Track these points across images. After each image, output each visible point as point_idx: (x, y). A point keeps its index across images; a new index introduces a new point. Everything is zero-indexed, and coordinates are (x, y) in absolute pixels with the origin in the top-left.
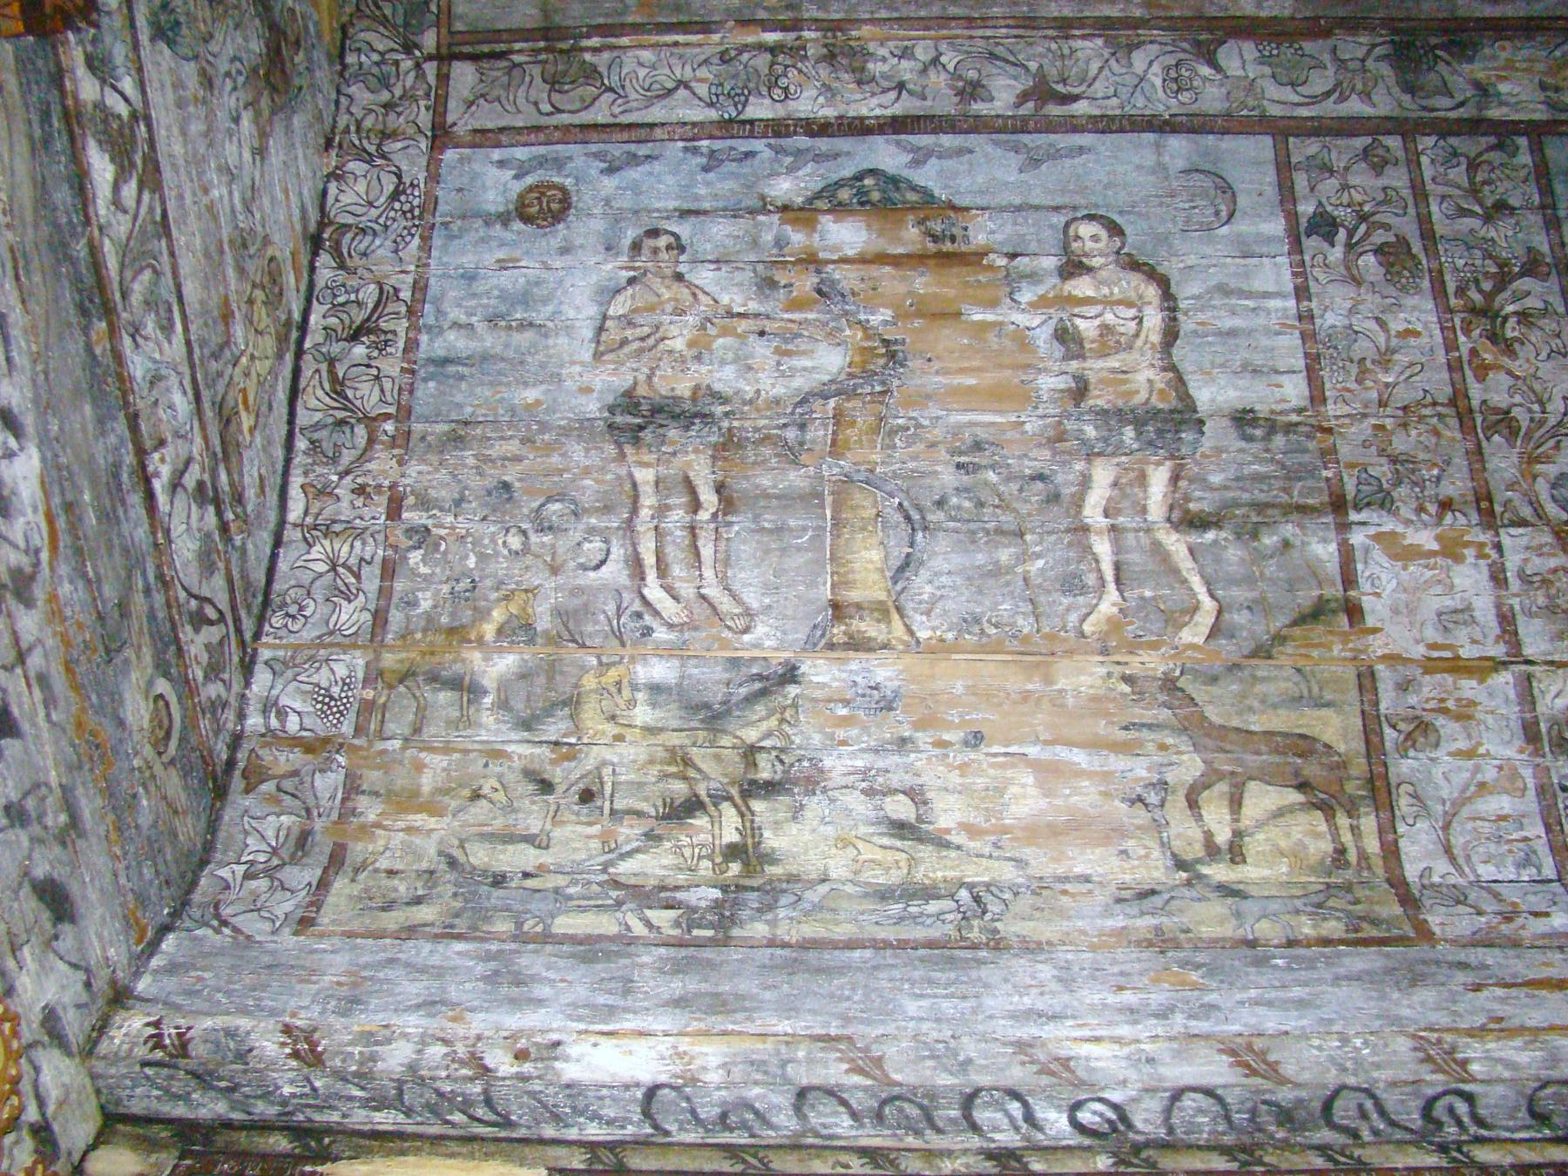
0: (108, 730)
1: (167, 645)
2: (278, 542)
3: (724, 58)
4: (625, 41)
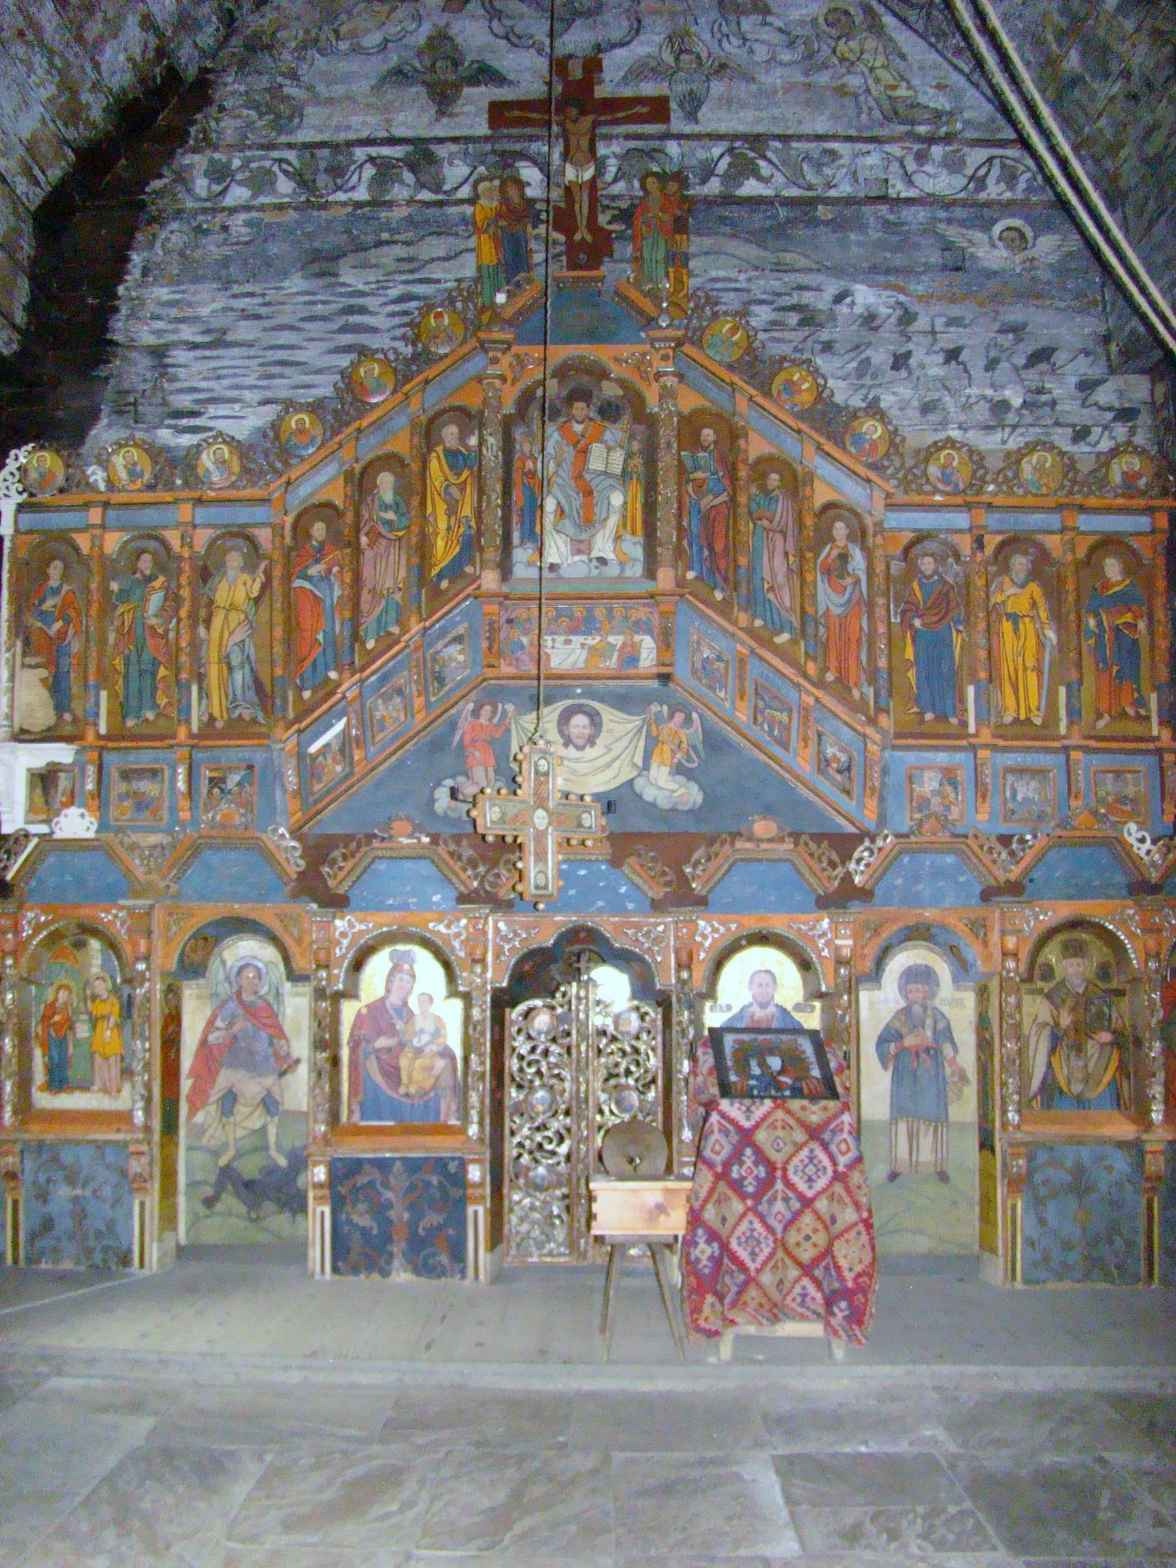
0: (993, 285)
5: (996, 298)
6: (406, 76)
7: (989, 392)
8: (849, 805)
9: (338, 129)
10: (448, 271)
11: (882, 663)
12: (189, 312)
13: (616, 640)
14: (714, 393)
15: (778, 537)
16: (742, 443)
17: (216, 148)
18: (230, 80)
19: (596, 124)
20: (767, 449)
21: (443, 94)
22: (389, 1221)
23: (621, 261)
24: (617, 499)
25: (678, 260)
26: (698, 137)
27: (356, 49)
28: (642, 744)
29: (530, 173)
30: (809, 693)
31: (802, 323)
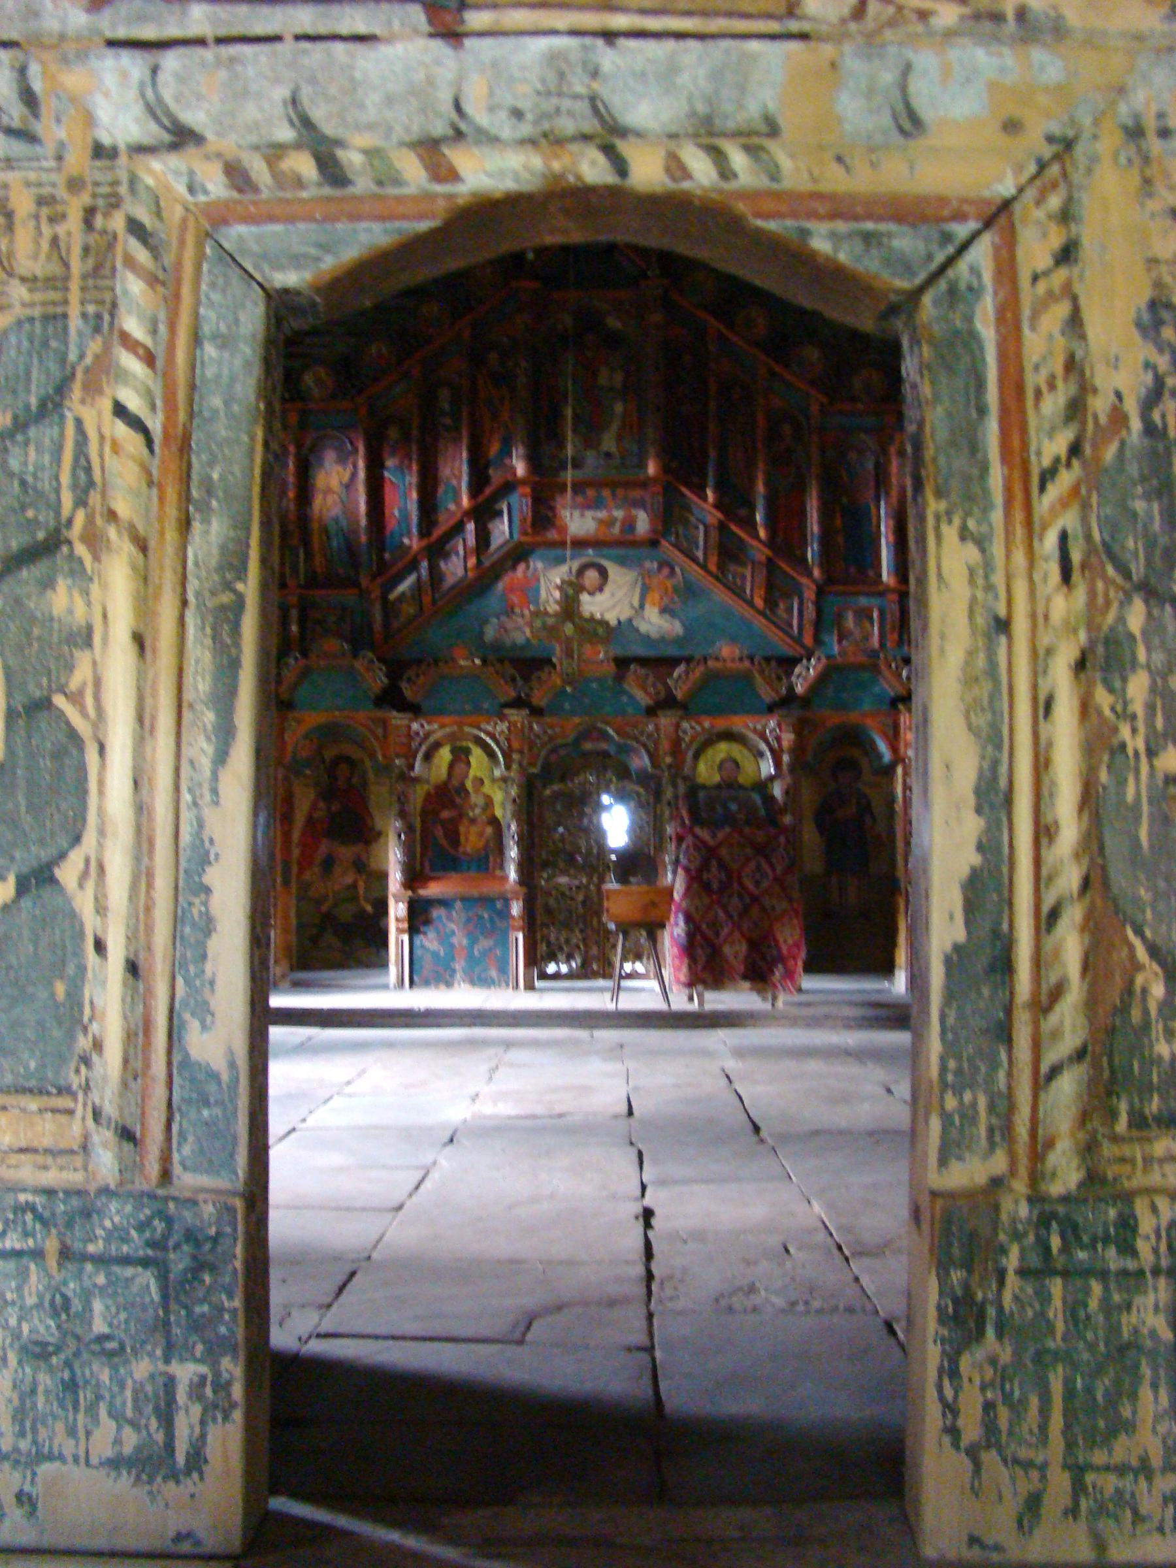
13: (619, 514)
22: (452, 946)
28: (638, 590)
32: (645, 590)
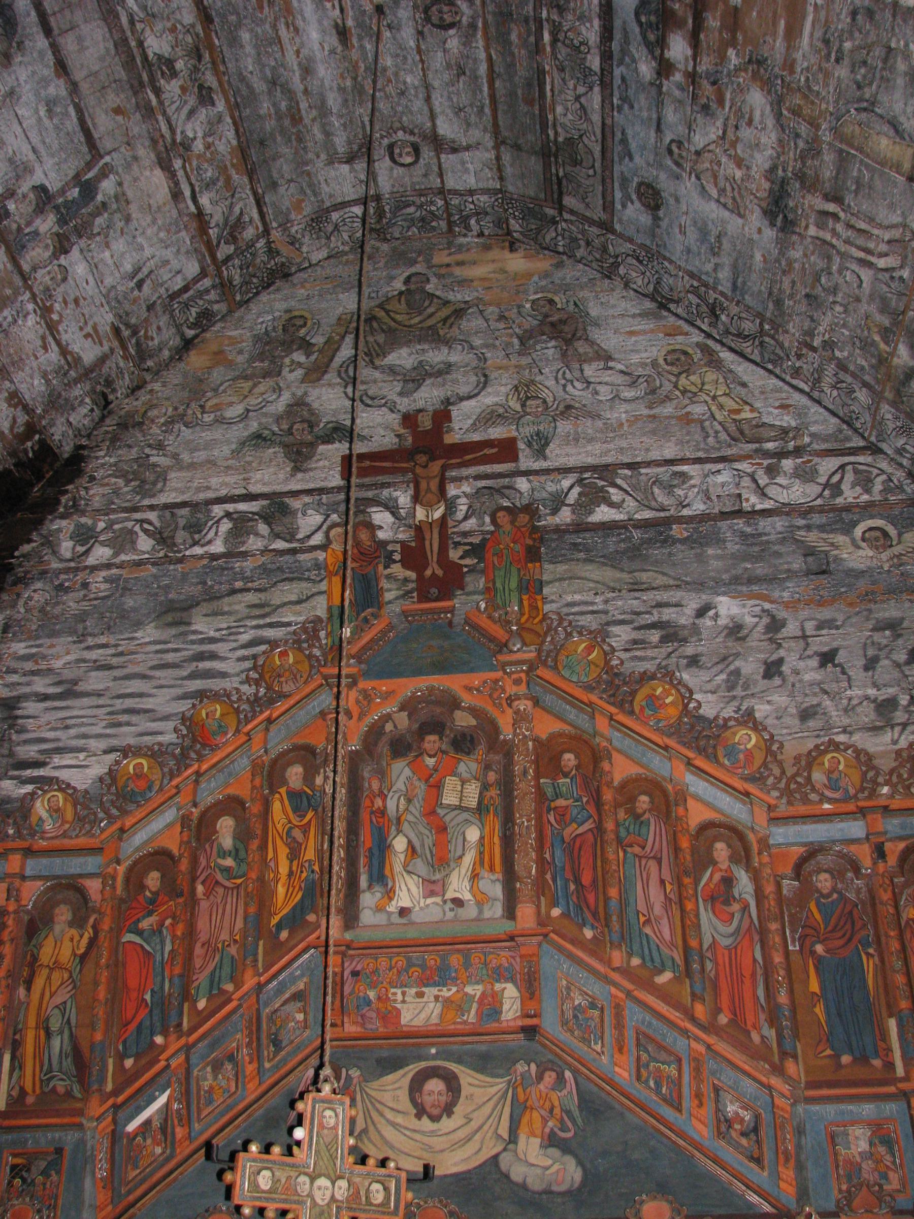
0: (862, 584)
1: (842, 520)
2: (819, 402)
3: (562, 69)
4: (550, 117)
5: (869, 597)
6: (265, 439)
7: (872, 692)
8: (761, 1177)
9: (198, 490)
10: (299, 614)
11: (783, 997)
12: (43, 665)
13: (474, 990)
14: (572, 714)
15: (652, 864)
16: (606, 765)
17: (83, 513)
18: (102, 453)
19: (444, 468)
20: (634, 770)
21: (299, 453)
23: (474, 593)
24: (473, 834)
25: (532, 588)
26: (547, 471)
27: (220, 421)
29: (381, 517)
30: (697, 1039)
31: (664, 640)
32: (519, 1111)
